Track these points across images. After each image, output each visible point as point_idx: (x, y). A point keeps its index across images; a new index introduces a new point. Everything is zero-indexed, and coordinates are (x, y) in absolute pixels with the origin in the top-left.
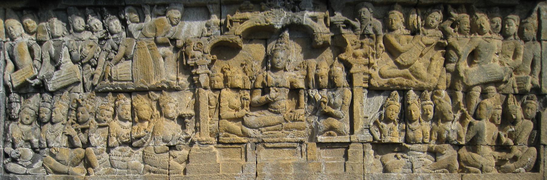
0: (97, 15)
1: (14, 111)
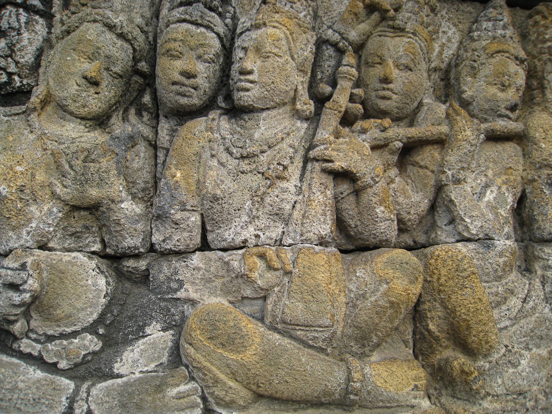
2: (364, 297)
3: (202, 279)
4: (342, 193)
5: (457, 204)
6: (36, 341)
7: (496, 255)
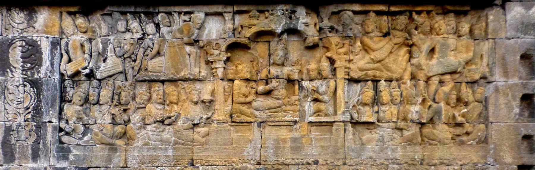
0: (136, 19)
1: (69, 94)
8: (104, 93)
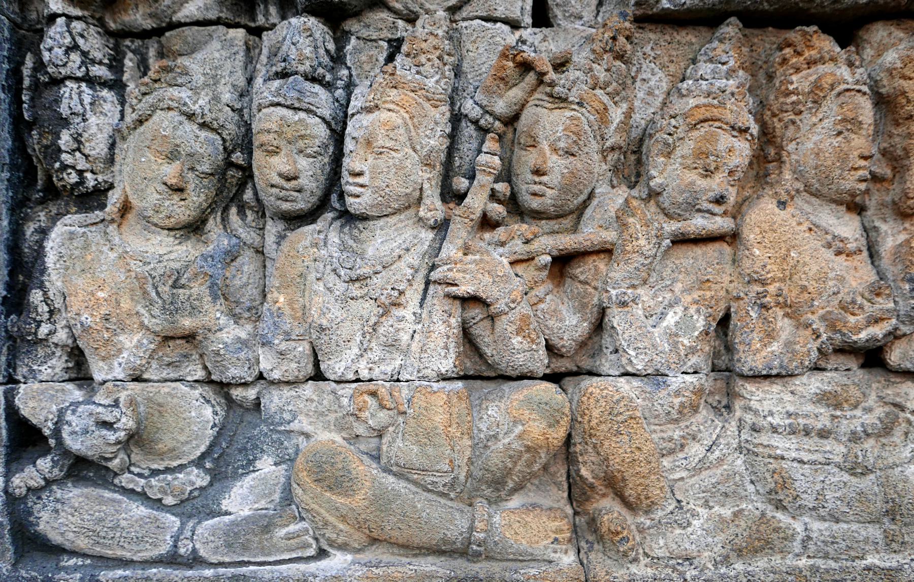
1: (77, 139)
2: (496, 438)
3: (315, 412)
4: (473, 319)
5: (620, 332)
6: (140, 475)
7: (669, 394)
8: (384, 115)
